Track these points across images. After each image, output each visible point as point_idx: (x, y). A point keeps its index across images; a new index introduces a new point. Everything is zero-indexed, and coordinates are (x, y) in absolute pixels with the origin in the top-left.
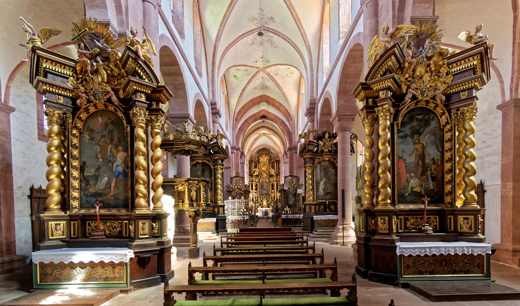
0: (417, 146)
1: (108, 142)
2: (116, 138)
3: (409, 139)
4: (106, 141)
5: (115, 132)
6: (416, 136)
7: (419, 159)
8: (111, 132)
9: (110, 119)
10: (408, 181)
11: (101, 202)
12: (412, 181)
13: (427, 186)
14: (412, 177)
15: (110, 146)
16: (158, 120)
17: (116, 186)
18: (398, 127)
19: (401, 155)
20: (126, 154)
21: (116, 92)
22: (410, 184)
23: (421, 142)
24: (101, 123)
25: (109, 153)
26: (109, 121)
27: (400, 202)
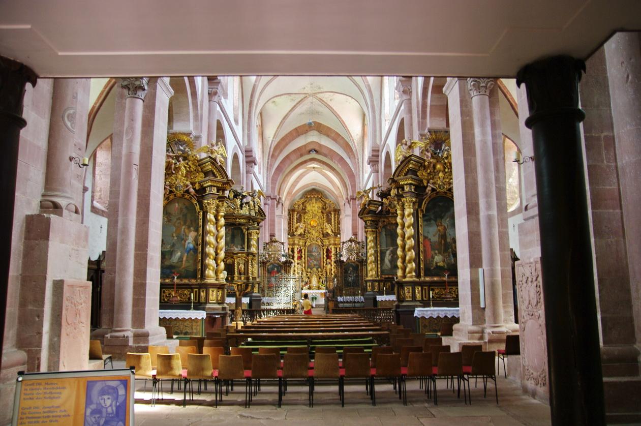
0: (440, 228)
1: (182, 223)
2: (189, 220)
3: (433, 222)
4: (180, 223)
5: (189, 216)
6: (438, 220)
7: (442, 238)
8: (185, 216)
9: (185, 205)
10: (433, 258)
11: (177, 273)
12: (436, 257)
13: (449, 261)
14: (436, 254)
15: (184, 227)
16: (223, 205)
17: (187, 260)
18: (423, 212)
19: (426, 235)
20: (196, 233)
21: (193, 184)
22: (435, 260)
23: (443, 224)
24: (177, 208)
25: (182, 233)
26: (184, 207)
27: (426, 275)
